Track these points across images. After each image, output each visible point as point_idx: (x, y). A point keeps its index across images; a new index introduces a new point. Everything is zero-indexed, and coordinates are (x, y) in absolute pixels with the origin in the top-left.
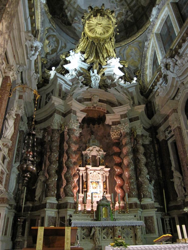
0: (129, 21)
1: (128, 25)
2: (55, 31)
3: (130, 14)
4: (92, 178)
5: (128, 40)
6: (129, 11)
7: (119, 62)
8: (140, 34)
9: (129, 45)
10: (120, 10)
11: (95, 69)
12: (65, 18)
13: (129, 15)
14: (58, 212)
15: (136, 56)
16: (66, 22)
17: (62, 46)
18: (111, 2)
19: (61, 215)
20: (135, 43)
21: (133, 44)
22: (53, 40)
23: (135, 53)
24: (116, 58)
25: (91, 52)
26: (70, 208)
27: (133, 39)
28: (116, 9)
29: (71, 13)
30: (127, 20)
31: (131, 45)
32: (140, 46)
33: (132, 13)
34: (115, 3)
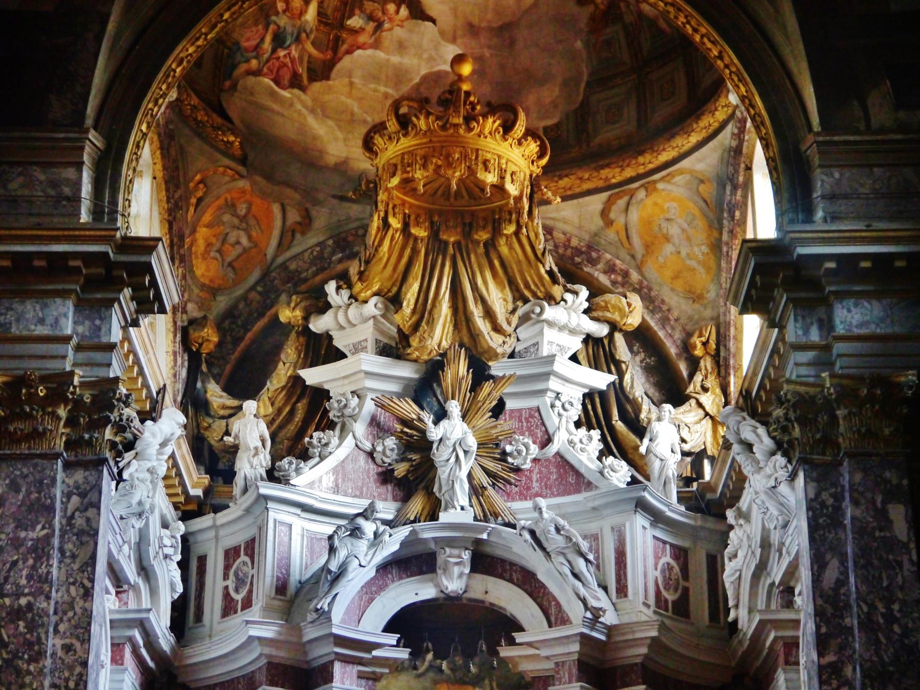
5: (641, 159)
7: (585, 312)
8: (694, 139)
11: (453, 398)
15: (689, 239)
17: (289, 223)
20: (678, 179)
21: (669, 182)
22: (238, 217)
23: (685, 226)
24: (569, 297)
25: (429, 307)
27: (664, 157)
30: (640, 14)
31: (660, 186)
32: (706, 196)
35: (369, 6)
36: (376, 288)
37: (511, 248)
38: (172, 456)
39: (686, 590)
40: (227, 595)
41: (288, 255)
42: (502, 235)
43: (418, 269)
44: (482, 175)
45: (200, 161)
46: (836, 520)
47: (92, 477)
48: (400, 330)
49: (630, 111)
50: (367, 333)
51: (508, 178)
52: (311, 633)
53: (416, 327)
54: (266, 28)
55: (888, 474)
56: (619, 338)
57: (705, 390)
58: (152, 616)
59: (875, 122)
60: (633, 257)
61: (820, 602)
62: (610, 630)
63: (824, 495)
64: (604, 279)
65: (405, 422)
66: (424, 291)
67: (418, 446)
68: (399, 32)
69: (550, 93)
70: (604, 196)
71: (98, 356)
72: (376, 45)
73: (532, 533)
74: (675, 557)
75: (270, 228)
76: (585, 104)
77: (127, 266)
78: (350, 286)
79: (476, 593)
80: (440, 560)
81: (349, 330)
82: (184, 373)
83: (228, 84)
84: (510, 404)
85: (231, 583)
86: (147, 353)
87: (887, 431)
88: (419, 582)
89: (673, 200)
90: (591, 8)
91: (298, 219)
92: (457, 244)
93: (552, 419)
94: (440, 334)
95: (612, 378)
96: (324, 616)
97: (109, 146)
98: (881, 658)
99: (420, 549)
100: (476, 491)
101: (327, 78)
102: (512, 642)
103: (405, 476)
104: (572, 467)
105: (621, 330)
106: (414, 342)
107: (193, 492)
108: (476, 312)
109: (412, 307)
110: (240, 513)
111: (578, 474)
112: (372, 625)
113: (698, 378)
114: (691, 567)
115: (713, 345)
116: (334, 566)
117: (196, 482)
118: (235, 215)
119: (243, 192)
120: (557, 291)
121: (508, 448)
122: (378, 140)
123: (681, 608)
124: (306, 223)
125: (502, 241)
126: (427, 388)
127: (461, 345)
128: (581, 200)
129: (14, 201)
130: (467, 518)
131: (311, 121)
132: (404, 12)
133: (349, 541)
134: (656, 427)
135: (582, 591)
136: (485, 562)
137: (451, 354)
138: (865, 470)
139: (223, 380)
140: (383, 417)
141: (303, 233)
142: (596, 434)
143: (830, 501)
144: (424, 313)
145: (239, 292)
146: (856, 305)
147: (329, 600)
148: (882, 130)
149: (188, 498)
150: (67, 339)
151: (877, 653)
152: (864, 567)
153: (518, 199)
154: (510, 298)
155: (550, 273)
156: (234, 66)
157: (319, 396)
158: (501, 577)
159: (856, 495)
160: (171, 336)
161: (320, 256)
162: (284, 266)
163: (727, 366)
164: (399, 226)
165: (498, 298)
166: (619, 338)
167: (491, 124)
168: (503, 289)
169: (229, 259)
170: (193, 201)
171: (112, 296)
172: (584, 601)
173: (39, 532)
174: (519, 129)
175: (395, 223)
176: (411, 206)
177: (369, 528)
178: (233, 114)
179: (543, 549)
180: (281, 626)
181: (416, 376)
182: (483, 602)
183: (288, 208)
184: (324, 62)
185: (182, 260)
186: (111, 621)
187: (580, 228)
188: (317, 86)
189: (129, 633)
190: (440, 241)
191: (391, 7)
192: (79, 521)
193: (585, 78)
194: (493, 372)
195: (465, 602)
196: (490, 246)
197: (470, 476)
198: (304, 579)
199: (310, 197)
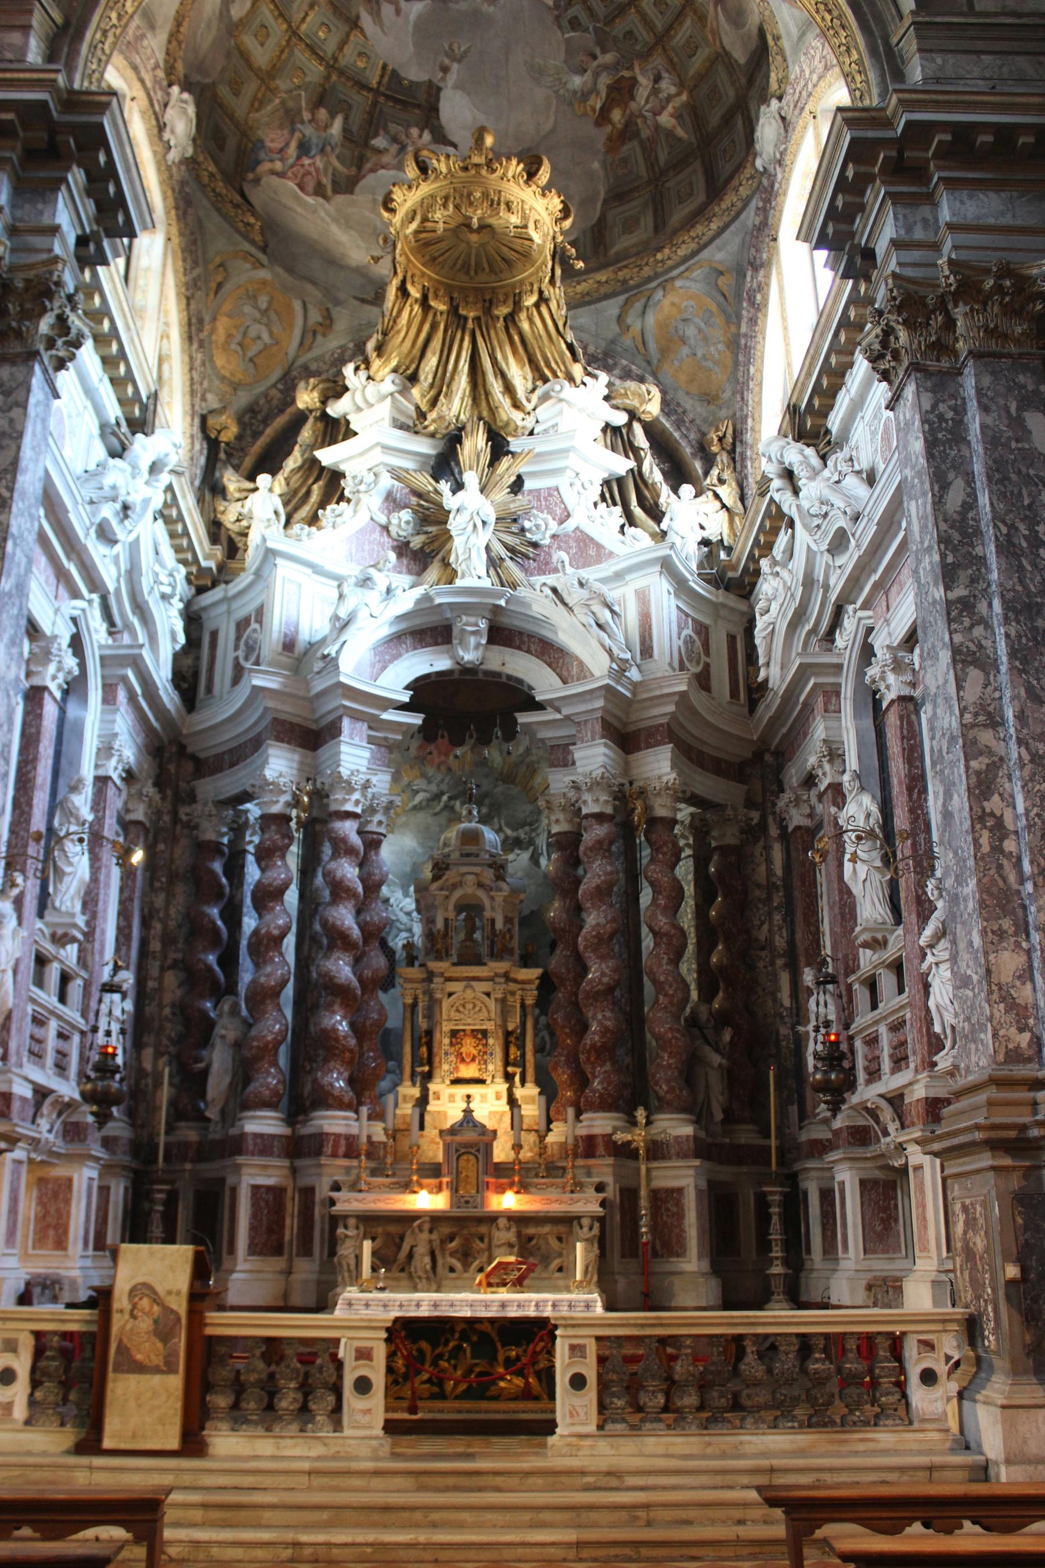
0: (670, 134)
1: (663, 155)
2: (264, 259)
3: (673, 90)
4: (458, 1016)
6: (665, 75)
7: (607, 398)
9: (669, 286)
10: (616, 66)
12: (318, 159)
13: (669, 99)
14: (294, 1171)
15: (705, 339)
16: (324, 181)
18: (565, 22)
19: (304, 1181)
20: (697, 273)
24: (587, 379)
26: (334, 1155)
28: (595, 63)
29: (346, 119)
30: (657, 127)
31: (678, 283)
33: (681, 85)
34: (586, 30)
35: (393, 128)
36: (394, 363)
37: (530, 319)
38: (170, 488)
39: (707, 666)
41: (310, 355)
42: (520, 310)
43: (436, 343)
46: (958, 435)
47: (19, 371)
48: (417, 408)
49: (648, 221)
50: (385, 410)
51: (531, 225)
52: (319, 685)
53: (434, 403)
54: (292, 132)
55: (1021, 379)
56: (637, 427)
57: (721, 481)
58: (146, 654)
60: (649, 363)
61: (943, 526)
62: (635, 686)
63: (942, 407)
66: (443, 362)
67: (432, 518)
70: (622, 298)
73: (554, 590)
75: (291, 326)
76: (602, 219)
77: (73, 128)
78: (367, 368)
80: (455, 632)
81: (367, 412)
82: (202, 461)
83: (251, 176)
84: (528, 485)
85: (241, 653)
86: (128, 328)
87: (1019, 330)
88: (435, 653)
89: (690, 298)
90: (608, 129)
91: (320, 319)
92: (477, 319)
93: (570, 498)
94: (456, 405)
95: (632, 464)
97: (67, 23)
98: (1026, 587)
100: (494, 563)
101: (352, 192)
103: (422, 549)
104: (592, 540)
105: (639, 420)
107: (204, 563)
108: (496, 387)
109: (430, 380)
110: (251, 578)
111: (599, 546)
113: (715, 472)
114: (713, 646)
115: (729, 439)
116: (343, 614)
117: (208, 556)
118: (256, 307)
119: (264, 283)
121: (527, 524)
124: (328, 322)
125: (523, 316)
126: (445, 464)
127: (480, 419)
128: (598, 305)
130: (486, 583)
131: (335, 229)
132: (427, 136)
133: (359, 590)
135: (607, 642)
136: (503, 633)
137: (469, 428)
138: (993, 373)
141: (324, 335)
142: (618, 510)
143: (950, 415)
145: (260, 389)
146: (971, 197)
147: (336, 647)
149: (202, 572)
151: (1021, 581)
152: (1000, 482)
153: (541, 247)
154: (530, 376)
155: (570, 347)
156: (258, 163)
158: (519, 648)
159: (985, 400)
160: (189, 419)
163: (743, 459)
164: (418, 295)
165: (519, 375)
166: (637, 427)
168: (522, 368)
169: (250, 354)
170: (214, 285)
171: (57, 174)
172: (610, 652)
174: (544, 175)
175: (415, 293)
176: (430, 278)
178: (253, 200)
179: (565, 604)
180: (286, 677)
181: (433, 452)
182: (499, 675)
183: (310, 307)
184: (348, 177)
185: (201, 344)
186: (102, 658)
187: (597, 335)
188: (340, 198)
189: (122, 672)
190: (460, 317)
191: (415, 132)
193: (602, 195)
194: (512, 448)
195: (481, 676)
196: (511, 319)
197: (488, 548)
198: (314, 640)
199: (332, 299)
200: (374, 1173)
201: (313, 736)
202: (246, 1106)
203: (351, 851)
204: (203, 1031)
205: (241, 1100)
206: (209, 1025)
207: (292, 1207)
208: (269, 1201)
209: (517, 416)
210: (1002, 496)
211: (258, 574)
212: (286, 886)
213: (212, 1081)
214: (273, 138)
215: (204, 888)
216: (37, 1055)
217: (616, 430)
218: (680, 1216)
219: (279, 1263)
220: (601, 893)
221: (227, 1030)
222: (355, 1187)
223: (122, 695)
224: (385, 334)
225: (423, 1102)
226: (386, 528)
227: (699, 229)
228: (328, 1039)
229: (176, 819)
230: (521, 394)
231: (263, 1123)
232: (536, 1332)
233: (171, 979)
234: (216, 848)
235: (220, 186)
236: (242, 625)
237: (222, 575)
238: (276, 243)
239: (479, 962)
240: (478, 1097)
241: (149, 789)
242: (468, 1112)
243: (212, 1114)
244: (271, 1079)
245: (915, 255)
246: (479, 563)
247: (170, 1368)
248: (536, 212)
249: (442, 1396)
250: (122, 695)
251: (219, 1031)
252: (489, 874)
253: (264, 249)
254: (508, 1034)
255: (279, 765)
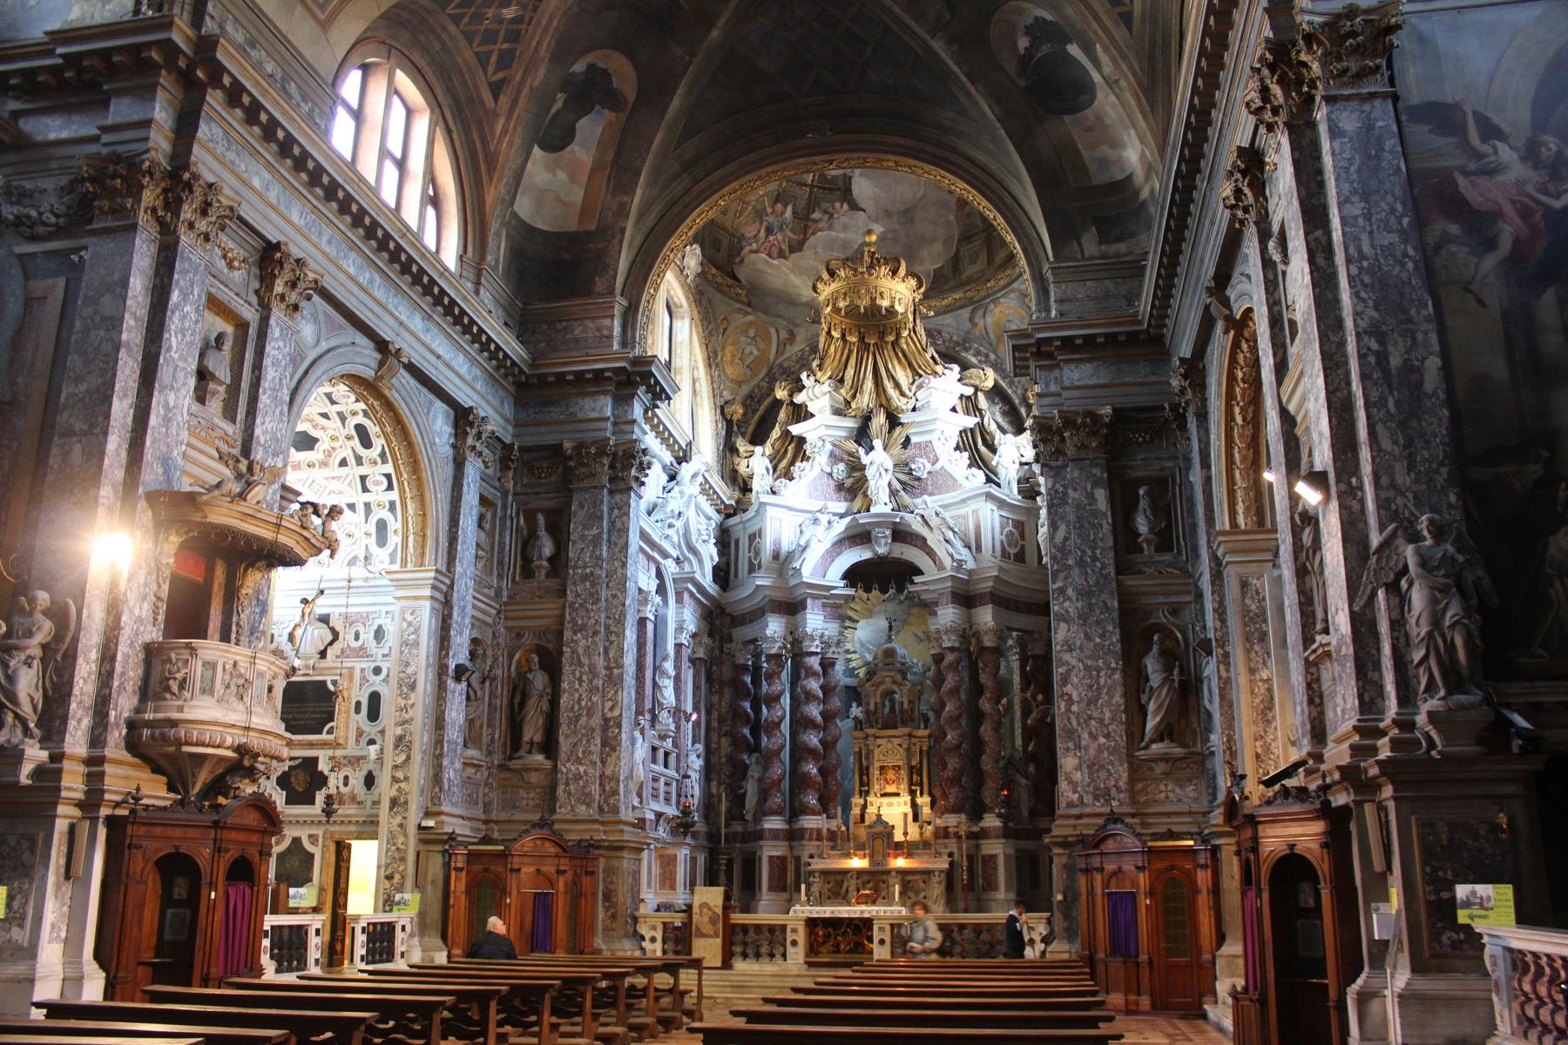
14: (791, 848)
19: (796, 853)
35: (824, 205)
39: (1023, 547)
40: (750, 562)
43: (852, 361)
44: (879, 302)
45: (723, 306)
46: (1064, 502)
52: (793, 582)
53: (854, 396)
56: (981, 396)
58: (698, 577)
59: (1087, 254)
62: (970, 572)
64: (974, 360)
65: (850, 454)
66: (857, 372)
67: (856, 467)
68: (843, 219)
69: (937, 248)
71: (626, 428)
72: (830, 228)
74: (1015, 526)
76: (957, 253)
77: (639, 374)
79: (896, 554)
84: (914, 440)
94: (866, 399)
95: (978, 420)
96: (798, 571)
99: (860, 530)
100: (893, 493)
102: (912, 583)
106: (853, 405)
108: (889, 385)
112: (834, 576)
116: (803, 543)
117: (727, 495)
120: (939, 369)
122: (819, 285)
123: (1020, 557)
124: (792, 338)
126: (862, 435)
129: (576, 340)
130: (888, 509)
132: (846, 206)
134: (1001, 450)
136: (901, 534)
139: (748, 436)
140: (837, 452)
142: (966, 455)
144: (856, 389)
145: (755, 382)
148: (1092, 258)
149: (726, 506)
150: (607, 419)
157: (801, 440)
161: (802, 358)
162: (781, 365)
165: (903, 376)
166: (981, 396)
167: (884, 270)
173: (595, 531)
174: (902, 271)
177: (824, 519)
178: (740, 277)
188: (794, 256)
191: (838, 205)
192: (618, 524)
196: (895, 344)
197: (890, 485)
200: (833, 848)
201: (792, 608)
202: (765, 814)
203: (815, 674)
204: (741, 771)
205: (762, 812)
206: (746, 768)
207: (791, 866)
208: (779, 864)
209: (904, 400)
210: (1080, 536)
211: (757, 511)
212: (782, 693)
213: (748, 799)
214: (749, 232)
215: (740, 691)
216: (655, 796)
217: (968, 398)
218: (995, 869)
219: (785, 896)
220: (954, 692)
221: (754, 772)
222: (821, 856)
223: (686, 596)
224: (821, 359)
225: (865, 807)
226: (830, 474)
227: (1009, 272)
228: (807, 775)
229: (722, 651)
230: (905, 388)
231: (774, 823)
232: (867, 923)
233: (725, 742)
234: (745, 668)
235: (719, 280)
236: (752, 537)
237: (740, 507)
238: (757, 298)
239: (895, 728)
240: (893, 808)
241: (706, 640)
242: (879, 816)
243: (749, 817)
244: (776, 800)
245: (1049, 400)
246: (884, 495)
247: (716, 935)
248: (899, 292)
249: (838, 951)
250: (686, 596)
251: (750, 773)
252: (898, 677)
253: (749, 305)
254: (912, 768)
255: (774, 627)
